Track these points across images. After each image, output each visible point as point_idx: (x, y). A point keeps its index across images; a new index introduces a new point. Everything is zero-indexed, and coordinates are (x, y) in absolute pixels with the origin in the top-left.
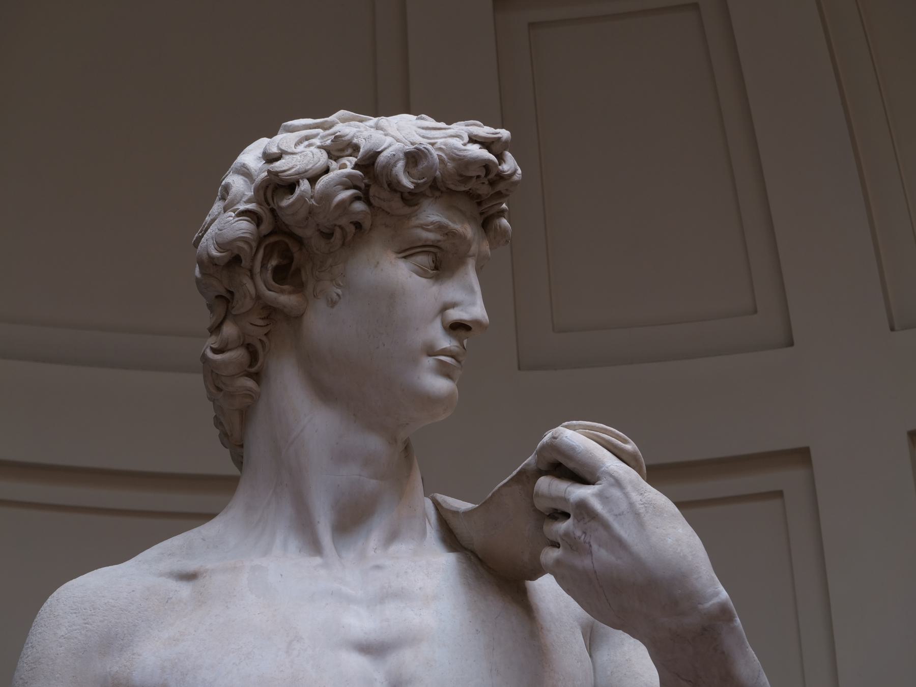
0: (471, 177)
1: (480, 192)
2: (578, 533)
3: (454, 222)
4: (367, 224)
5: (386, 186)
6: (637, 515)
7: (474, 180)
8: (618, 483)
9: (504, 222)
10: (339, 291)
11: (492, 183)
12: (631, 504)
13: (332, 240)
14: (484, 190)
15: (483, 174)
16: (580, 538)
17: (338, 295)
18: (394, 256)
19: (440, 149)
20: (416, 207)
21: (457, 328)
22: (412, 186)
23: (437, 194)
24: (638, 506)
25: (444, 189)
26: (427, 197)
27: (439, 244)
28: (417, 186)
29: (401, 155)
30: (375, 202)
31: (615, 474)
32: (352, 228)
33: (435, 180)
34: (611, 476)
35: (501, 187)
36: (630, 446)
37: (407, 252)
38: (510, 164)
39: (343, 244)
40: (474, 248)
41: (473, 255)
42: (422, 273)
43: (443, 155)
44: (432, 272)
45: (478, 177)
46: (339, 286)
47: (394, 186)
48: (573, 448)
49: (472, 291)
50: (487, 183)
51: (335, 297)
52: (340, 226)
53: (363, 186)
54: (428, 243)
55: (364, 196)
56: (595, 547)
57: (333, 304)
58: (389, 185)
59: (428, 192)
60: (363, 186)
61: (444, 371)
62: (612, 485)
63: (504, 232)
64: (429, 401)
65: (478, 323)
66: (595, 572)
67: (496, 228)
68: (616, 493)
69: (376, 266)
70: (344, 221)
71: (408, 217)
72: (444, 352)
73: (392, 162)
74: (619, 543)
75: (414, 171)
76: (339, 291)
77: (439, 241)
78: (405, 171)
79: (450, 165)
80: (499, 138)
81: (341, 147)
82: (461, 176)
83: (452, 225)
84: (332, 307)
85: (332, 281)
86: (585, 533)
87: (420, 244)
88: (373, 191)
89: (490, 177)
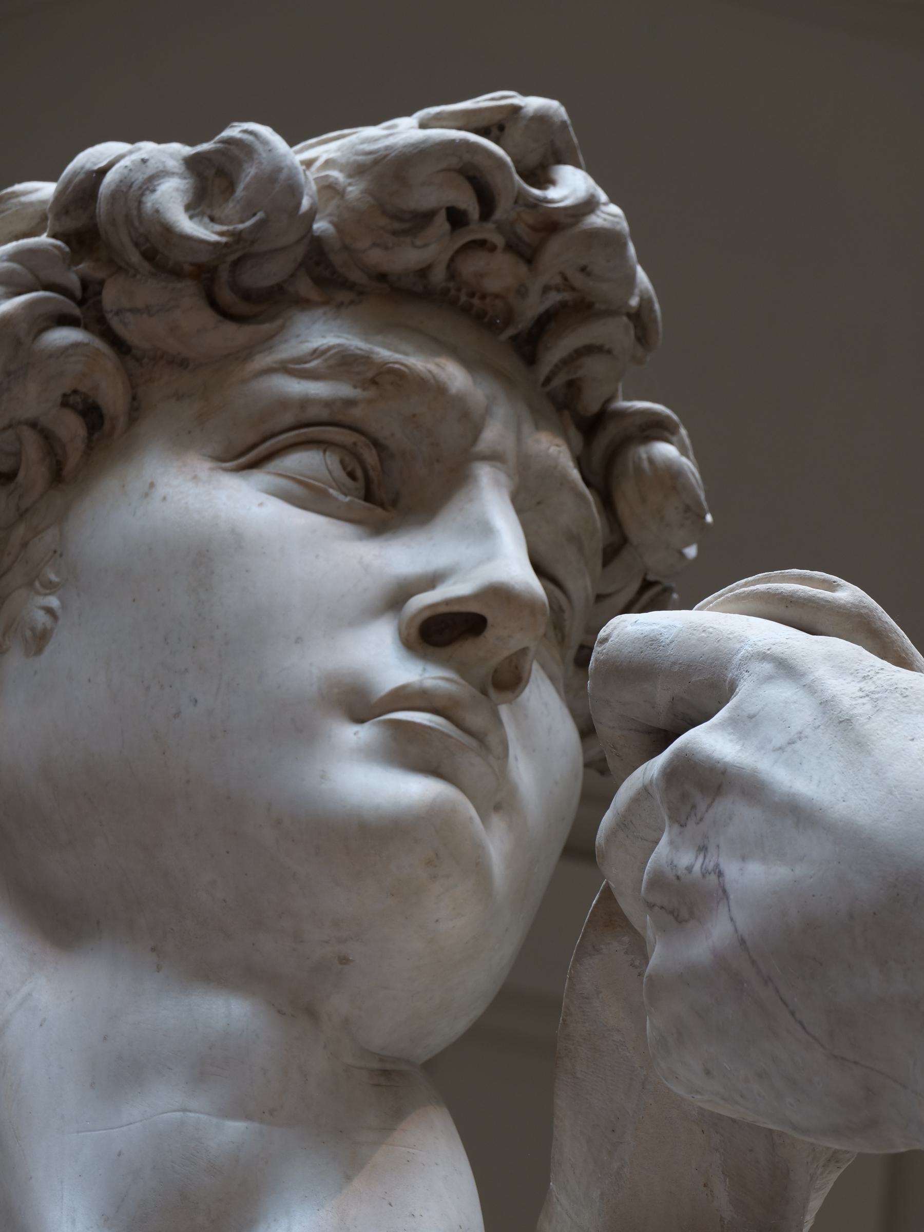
0: (425, 218)
1: (493, 285)
2: (686, 859)
3: (406, 354)
4: (112, 394)
5: (135, 257)
6: (842, 724)
7: (441, 224)
8: (785, 668)
9: (666, 450)
10: (53, 602)
11: (528, 256)
12: (826, 705)
13: (21, 474)
14: (497, 272)
15: (468, 202)
16: (689, 869)
17: (49, 611)
18: (208, 465)
19: (328, 164)
20: (266, 327)
21: (442, 631)
22: (214, 238)
23: (343, 296)
24: (846, 702)
25: (356, 276)
26: (304, 304)
27: (357, 413)
28: (239, 251)
29: (173, 164)
30: (131, 329)
31: (777, 650)
32: (71, 428)
33: (317, 243)
34: (764, 657)
35: (557, 256)
36: (848, 593)
37: (248, 454)
38: (571, 184)
39: (58, 476)
40: (494, 434)
41: (494, 457)
42: (309, 497)
43: (336, 174)
44: (341, 497)
45: (456, 218)
46: (51, 587)
47: (159, 249)
48: (652, 641)
49: (486, 531)
50: (498, 240)
51: (41, 618)
52: (33, 425)
53: (72, 280)
54: (313, 413)
55: (85, 306)
56: (732, 870)
57: (39, 641)
58: (150, 255)
59: (304, 287)
60: (72, 280)
61: (410, 751)
62: (769, 678)
63: (670, 477)
64: (373, 838)
65: (500, 594)
66: (742, 942)
67: (638, 469)
68: (780, 693)
69: (146, 495)
70: (33, 399)
71: (247, 353)
72: (404, 698)
73: (140, 177)
74: (797, 814)
75: (230, 208)
76: (53, 602)
77: (350, 403)
78: (194, 208)
79: (354, 190)
80: (516, 109)
81: (21, 227)
82: (397, 216)
83: (384, 353)
84: (39, 651)
85: (30, 584)
86: (703, 849)
87: (288, 419)
88: (111, 297)
89: (498, 215)
